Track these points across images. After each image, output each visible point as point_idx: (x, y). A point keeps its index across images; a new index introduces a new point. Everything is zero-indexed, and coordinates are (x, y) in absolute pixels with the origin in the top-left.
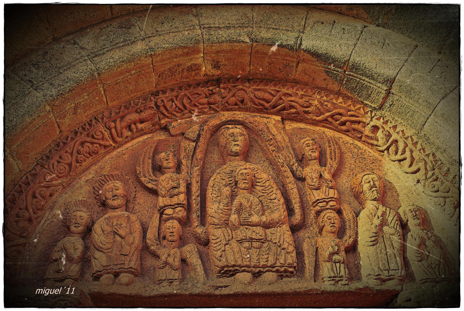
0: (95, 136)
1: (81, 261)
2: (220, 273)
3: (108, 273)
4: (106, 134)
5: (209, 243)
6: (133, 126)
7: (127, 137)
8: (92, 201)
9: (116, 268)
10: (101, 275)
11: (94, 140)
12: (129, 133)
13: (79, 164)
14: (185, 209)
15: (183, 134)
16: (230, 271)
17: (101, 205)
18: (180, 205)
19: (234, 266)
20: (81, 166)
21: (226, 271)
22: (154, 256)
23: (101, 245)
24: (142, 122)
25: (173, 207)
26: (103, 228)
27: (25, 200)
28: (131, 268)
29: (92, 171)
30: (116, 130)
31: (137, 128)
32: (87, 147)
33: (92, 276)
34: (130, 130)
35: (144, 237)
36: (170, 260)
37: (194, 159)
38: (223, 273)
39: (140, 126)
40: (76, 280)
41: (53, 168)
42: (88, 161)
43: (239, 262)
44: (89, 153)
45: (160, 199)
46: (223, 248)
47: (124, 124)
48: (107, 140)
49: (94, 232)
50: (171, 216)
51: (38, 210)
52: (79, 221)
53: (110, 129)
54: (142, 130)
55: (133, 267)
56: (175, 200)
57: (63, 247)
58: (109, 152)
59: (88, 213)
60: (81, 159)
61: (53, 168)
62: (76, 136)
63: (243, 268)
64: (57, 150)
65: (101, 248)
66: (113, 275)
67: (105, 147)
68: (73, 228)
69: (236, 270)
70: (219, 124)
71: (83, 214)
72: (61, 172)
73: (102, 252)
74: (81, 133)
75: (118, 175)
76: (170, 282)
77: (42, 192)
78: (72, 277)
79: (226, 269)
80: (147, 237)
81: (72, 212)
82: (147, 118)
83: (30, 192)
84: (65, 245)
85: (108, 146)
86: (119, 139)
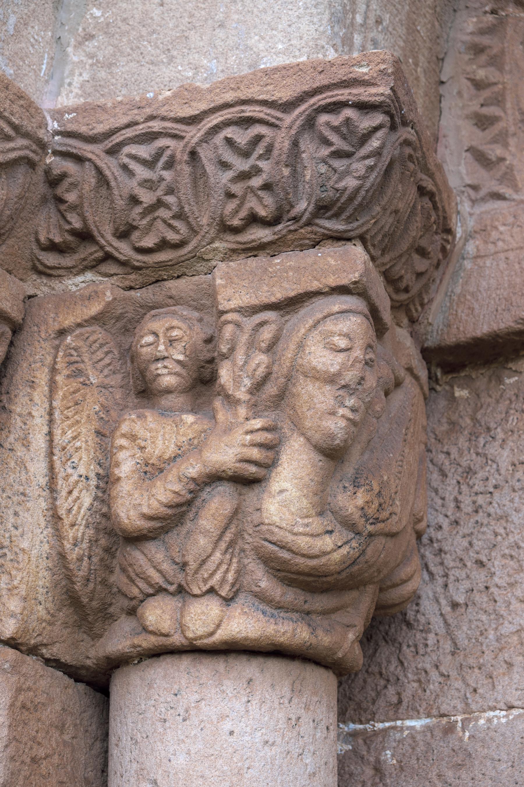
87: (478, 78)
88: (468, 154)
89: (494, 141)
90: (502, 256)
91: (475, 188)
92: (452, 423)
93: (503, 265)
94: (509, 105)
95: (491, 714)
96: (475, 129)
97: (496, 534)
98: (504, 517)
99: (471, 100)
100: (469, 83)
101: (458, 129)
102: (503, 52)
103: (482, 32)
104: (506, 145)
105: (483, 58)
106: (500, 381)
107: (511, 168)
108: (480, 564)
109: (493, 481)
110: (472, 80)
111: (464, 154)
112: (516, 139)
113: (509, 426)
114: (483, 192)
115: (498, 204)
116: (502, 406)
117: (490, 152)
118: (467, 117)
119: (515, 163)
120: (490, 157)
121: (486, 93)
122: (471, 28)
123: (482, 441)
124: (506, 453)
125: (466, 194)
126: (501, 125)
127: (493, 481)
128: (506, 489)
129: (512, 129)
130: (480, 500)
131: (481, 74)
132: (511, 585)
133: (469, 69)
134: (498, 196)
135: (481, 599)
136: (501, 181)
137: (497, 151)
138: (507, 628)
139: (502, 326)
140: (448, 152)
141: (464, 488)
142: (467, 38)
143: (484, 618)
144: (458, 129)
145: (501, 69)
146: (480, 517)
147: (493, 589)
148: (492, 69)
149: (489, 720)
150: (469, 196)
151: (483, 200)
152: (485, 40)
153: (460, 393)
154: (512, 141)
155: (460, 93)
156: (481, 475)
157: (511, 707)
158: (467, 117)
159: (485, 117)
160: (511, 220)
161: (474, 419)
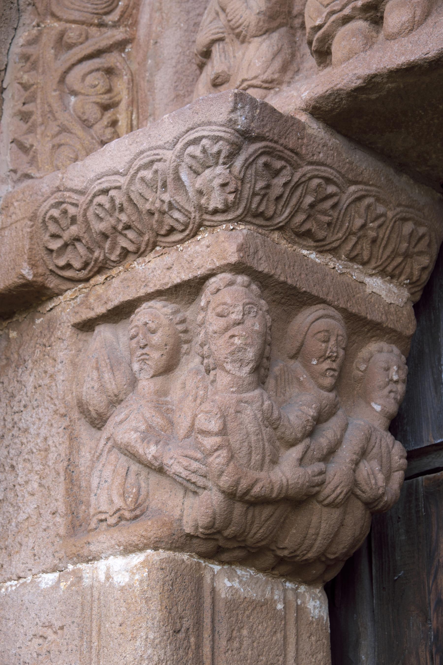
3: (346, 20)
66: (366, 20)
78: (254, 82)
87: (24, 81)
90: (14, 226)
92: (8, 359)
93: (14, 234)
95: (9, 583)
96: (21, 123)
97: (22, 444)
98: (26, 430)
100: (20, 87)
106: (34, 322)
108: (13, 467)
109: (23, 403)
110: (21, 84)
111: (10, 146)
112: (43, 128)
113: (35, 358)
115: (30, 182)
116: (32, 344)
117: (26, 141)
120: (26, 145)
123: (20, 370)
124: (32, 379)
125: (10, 177)
126: (34, 117)
127: (23, 403)
128: (30, 408)
130: (16, 417)
131: (26, 78)
132: (27, 482)
133: (19, 76)
135: (10, 495)
137: (28, 140)
138: (22, 517)
139: (11, 282)
141: (9, 409)
143: (11, 509)
146: (15, 432)
147: (17, 487)
149: (7, 589)
150: (12, 178)
151: (20, 180)
152: (30, 50)
153: (13, 334)
156: (17, 399)
157: (19, 578)
159: (25, 113)
160: (21, 196)
161: (19, 355)
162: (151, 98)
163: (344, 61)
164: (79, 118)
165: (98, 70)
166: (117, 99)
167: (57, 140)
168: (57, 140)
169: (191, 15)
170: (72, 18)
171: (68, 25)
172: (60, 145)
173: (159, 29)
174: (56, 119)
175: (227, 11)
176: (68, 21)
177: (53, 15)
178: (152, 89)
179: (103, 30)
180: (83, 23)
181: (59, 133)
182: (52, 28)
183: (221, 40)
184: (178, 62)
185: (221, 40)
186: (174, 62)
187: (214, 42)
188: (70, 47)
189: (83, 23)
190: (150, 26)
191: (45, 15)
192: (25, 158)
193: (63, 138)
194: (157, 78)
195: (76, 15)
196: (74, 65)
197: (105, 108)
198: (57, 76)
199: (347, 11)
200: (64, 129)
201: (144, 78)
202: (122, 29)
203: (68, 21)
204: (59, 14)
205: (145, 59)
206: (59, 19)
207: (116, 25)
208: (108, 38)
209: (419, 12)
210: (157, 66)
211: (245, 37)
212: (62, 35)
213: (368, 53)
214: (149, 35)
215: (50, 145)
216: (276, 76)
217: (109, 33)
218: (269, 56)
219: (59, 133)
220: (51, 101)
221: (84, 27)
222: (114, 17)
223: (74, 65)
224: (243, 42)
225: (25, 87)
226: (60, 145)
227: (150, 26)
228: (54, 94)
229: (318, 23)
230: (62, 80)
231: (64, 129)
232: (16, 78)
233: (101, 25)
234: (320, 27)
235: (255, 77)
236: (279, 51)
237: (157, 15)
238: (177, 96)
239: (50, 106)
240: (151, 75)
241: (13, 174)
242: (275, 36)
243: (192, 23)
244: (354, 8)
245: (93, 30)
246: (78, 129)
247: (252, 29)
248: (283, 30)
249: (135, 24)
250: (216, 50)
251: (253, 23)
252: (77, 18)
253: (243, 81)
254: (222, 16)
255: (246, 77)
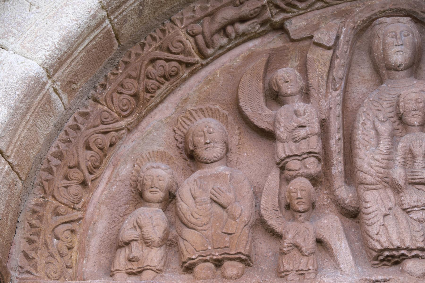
0: (172, 49)
1: (164, 244)
2: (377, 259)
3: (206, 261)
4: (190, 43)
5: (358, 213)
6: (230, 29)
7: (221, 47)
8: (173, 152)
9: (217, 255)
10: (195, 264)
11: (170, 55)
12: (224, 41)
13: (150, 95)
14: (319, 160)
15: (311, 37)
16: (393, 256)
17: (187, 158)
18: (311, 155)
19: (399, 249)
20: (152, 97)
21: (387, 256)
22: (274, 235)
23: (193, 220)
24: (243, 20)
25: (300, 158)
26: (193, 193)
27: (76, 154)
28: (240, 253)
29: (170, 105)
30: (204, 37)
31: (236, 32)
32: (161, 68)
33: (182, 267)
34: (227, 35)
35: (257, 205)
36: (299, 241)
37: (331, 78)
38: (382, 261)
39: (241, 27)
40: (158, 271)
41: (113, 103)
42: (163, 87)
43: (408, 244)
44: (164, 77)
45: (280, 146)
46: (381, 222)
47: (216, 26)
48: (189, 54)
49: (179, 198)
50: (297, 172)
51: (95, 168)
52: (157, 183)
53: (194, 36)
54: (244, 34)
55: (242, 251)
56: (304, 147)
57: (136, 224)
58: (193, 73)
59: (168, 171)
60: (152, 86)
61: (113, 103)
62: (143, 50)
63: (414, 253)
64: (117, 74)
65: (193, 223)
66: (214, 264)
67: (188, 65)
68: (148, 194)
69: (403, 255)
70: (370, 18)
71: (162, 172)
72: (125, 108)
73: (195, 229)
74: (150, 46)
75: (211, 109)
76: (300, 274)
77: (99, 141)
78: (153, 268)
79: (387, 253)
80: (262, 206)
81: (145, 169)
82: (251, 15)
83: (82, 142)
84: (139, 221)
85: (192, 64)
86: (210, 51)
87: (32, 223)
88: (22, 253)
89: (33, 250)
91: (22, 268)
94: (41, 237)
96: (27, 243)
99: (27, 232)
100: (28, 224)
101: (20, 242)
102: (43, 215)
103: (37, 205)
104: (37, 253)
105: (35, 216)
107: (36, 262)
110: (30, 224)
111: (20, 253)
112: (41, 251)
114: (24, 270)
115: (29, 276)
117: (30, 254)
118: (25, 238)
119: (38, 261)
120: (30, 256)
121: (34, 230)
122: (33, 203)
125: (18, 269)
126: (37, 244)
129: (40, 247)
131: (33, 222)
133: (29, 219)
134: (29, 272)
136: (32, 267)
137: (32, 254)
140: (14, 251)
142: (31, 206)
144: (20, 242)
145: (41, 222)
148: (38, 221)
150: (19, 270)
151: (23, 273)
152: (38, 209)
154: (39, 252)
155: (24, 228)
158: (25, 238)
159: (31, 240)
162: (87, 249)
163: (203, 279)
164: (59, 252)
165: (69, 230)
166: (73, 245)
167: (48, 260)
168: (48, 260)
169: (113, 216)
170: (63, 202)
171: (60, 204)
172: (49, 263)
173: (97, 218)
174: (48, 249)
175: (143, 229)
176: (60, 202)
177: (54, 197)
178: (89, 245)
179: (74, 211)
180: (67, 205)
181: (49, 256)
182: (53, 203)
183: (137, 240)
184: (103, 237)
185: (137, 240)
186: (101, 235)
187: (133, 240)
188: (58, 214)
189: (67, 205)
190: (93, 215)
191: (49, 195)
192: (26, 262)
193: (51, 259)
194: (92, 240)
195: (65, 201)
196: (60, 224)
197: (69, 248)
198: (51, 228)
199: (208, 258)
200: (51, 255)
201: (85, 238)
202: (81, 212)
203: (60, 202)
204: (57, 198)
205: (88, 229)
206: (56, 200)
207: (79, 210)
208: (76, 216)
209: (240, 272)
210: (93, 235)
211: (150, 245)
212: (56, 207)
213: (215, 280)
214: (92, 218)
215: (44, 262)
216: (162, 268)
217: (76, 213)
218: (161, 258)
219: (49, 256)
220: (48, 239)
221: (67, 207)
222: (78, 206)
223: (60, 224)
224: (148, 246)
225: (32, 226)
226: (49, 263)
227: (93, 215)
228: (49, 236)
229: (193, 257)
230: (53, 231)
231: (51, 255)
232: (27, 220)
233: (74, 208)
234: (193, 259)
235: (154, 267)
236: (164, 256)
237: (98, 211)
238: (99, 252)
239: (46, 241)
240: (90, 238)
241: (20, 269)
242: (163, 248)
243: (112, 220)
244: (211, 258)
245: (70, 210)
246: (58, 256)
247: (156, 243)
248: (164, 245)
249: (85, 211)
250: (133, 244)
251: (157, 241)
252: (65, 203)
253: (148, 265)
254: (138, 230)
255: (149, 264)
